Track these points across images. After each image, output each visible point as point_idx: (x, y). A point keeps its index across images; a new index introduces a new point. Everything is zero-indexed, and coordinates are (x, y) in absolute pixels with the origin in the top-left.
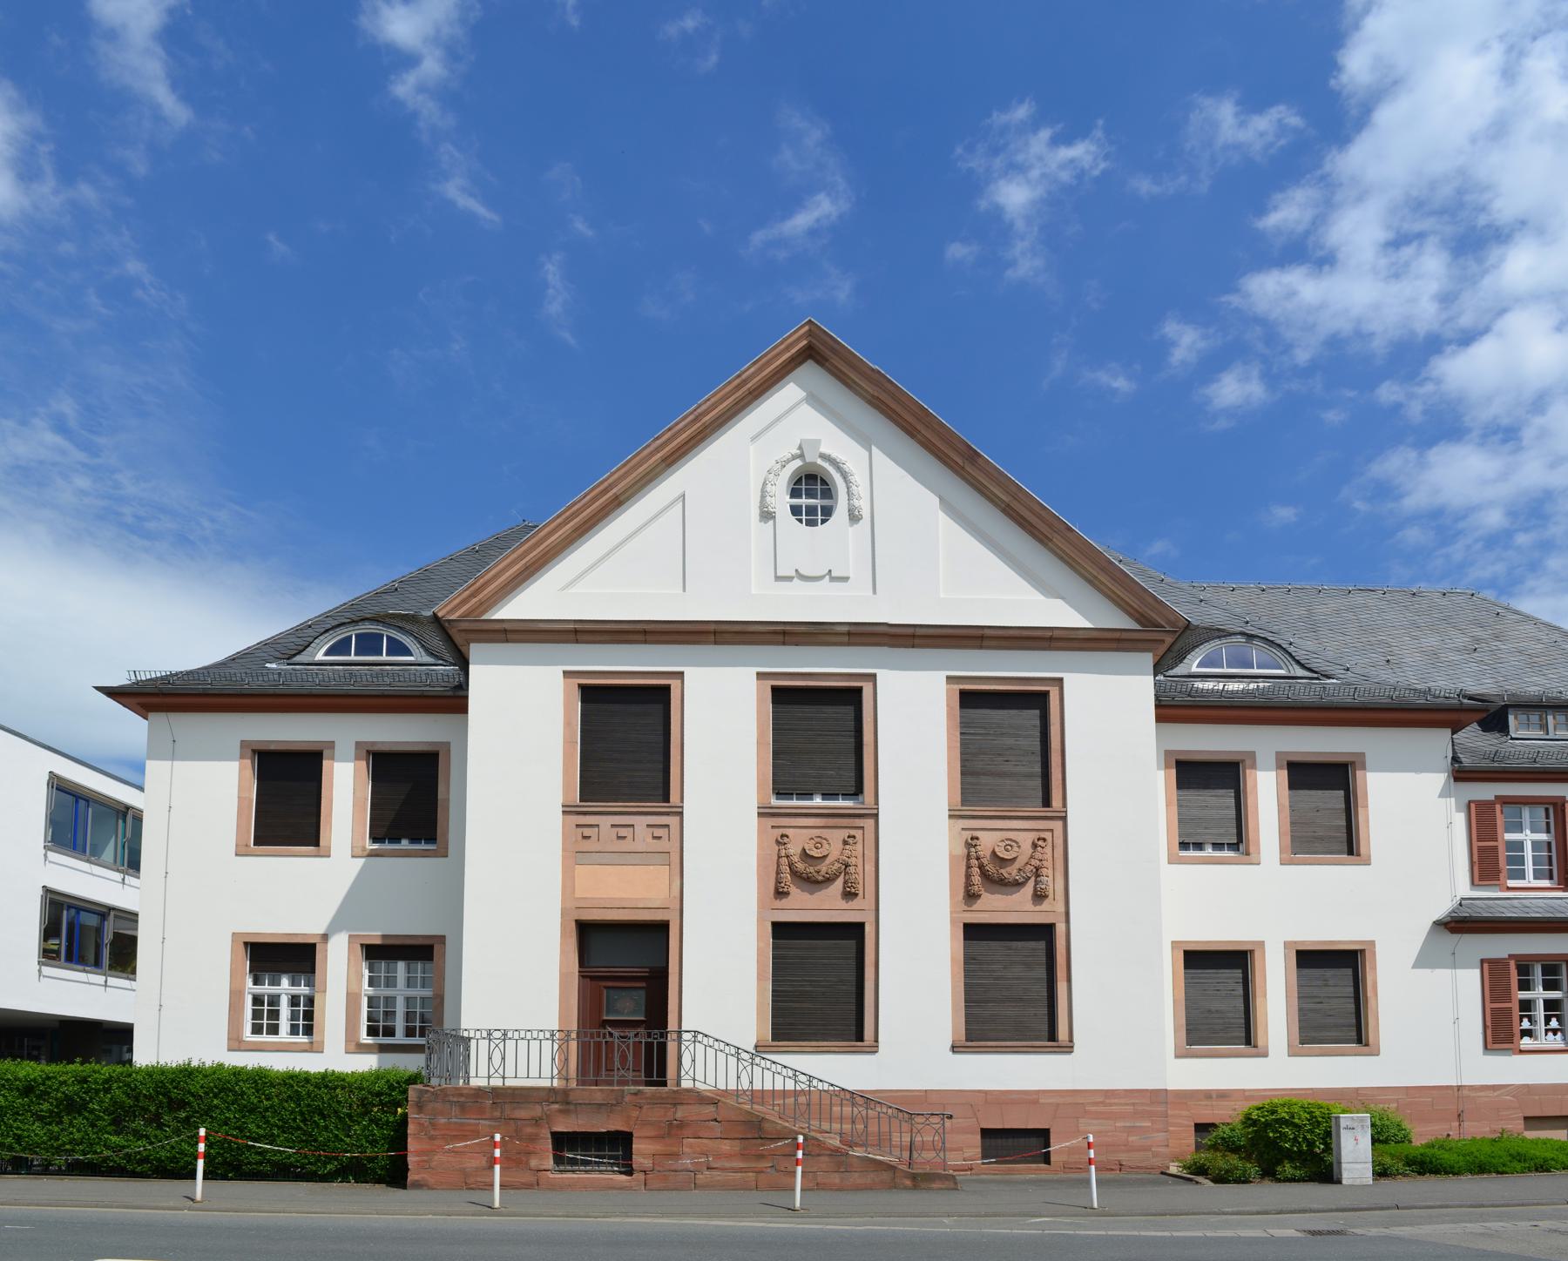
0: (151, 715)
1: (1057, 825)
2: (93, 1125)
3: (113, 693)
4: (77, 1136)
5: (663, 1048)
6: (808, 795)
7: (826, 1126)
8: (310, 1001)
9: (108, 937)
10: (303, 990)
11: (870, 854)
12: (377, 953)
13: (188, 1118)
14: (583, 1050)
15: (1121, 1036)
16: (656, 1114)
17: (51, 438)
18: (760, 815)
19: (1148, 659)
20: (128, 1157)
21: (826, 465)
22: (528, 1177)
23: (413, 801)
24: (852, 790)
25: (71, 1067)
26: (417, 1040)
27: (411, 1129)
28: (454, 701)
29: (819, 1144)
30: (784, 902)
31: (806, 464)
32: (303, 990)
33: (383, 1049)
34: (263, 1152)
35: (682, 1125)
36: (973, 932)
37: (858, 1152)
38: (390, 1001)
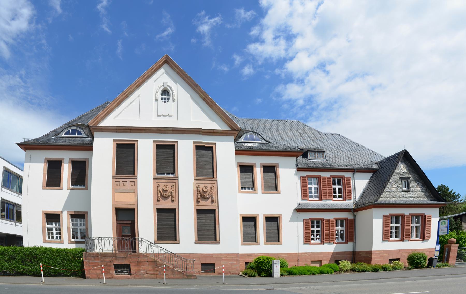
0: (27, 151)
1: (215, 182)
2: (18, 263)
3: (19, 144)
4: (15, 266)
5: (135, 242)
6: (163, 174)
7: (170, 263)
8: (60, 230)
9: (15, 212)
10: (58, 226)
11: (177, 190)
12: (74, 216)
13: (37, 261)
14: (118, 242)
15: (230, 242)
16: (135, 260)
17: (18, 80)
18: (154, 179)
19: (233, 138)
20: (27, 271)
21: (168, 88)
22: (110, 276)
23: (81, 176)
24: (173, 172)
25: (11, 247)
26: (83, 240)
27: (85, 263)
28: (89, 147)
29: (169, 267)
30: (159, 203)
31: (165, 88)
32: (58, 226)
33: (76, 242)
34: (55, 270)
35: (140, 262)
36: (199, 211)
37: (176, 269)
38: (77, 229)
